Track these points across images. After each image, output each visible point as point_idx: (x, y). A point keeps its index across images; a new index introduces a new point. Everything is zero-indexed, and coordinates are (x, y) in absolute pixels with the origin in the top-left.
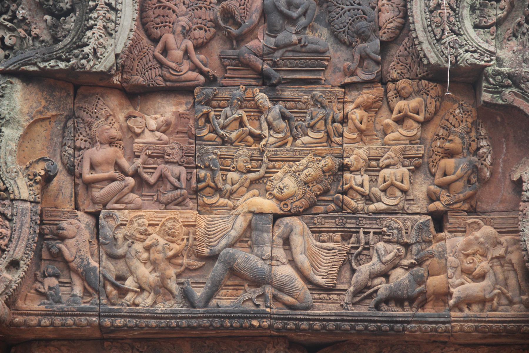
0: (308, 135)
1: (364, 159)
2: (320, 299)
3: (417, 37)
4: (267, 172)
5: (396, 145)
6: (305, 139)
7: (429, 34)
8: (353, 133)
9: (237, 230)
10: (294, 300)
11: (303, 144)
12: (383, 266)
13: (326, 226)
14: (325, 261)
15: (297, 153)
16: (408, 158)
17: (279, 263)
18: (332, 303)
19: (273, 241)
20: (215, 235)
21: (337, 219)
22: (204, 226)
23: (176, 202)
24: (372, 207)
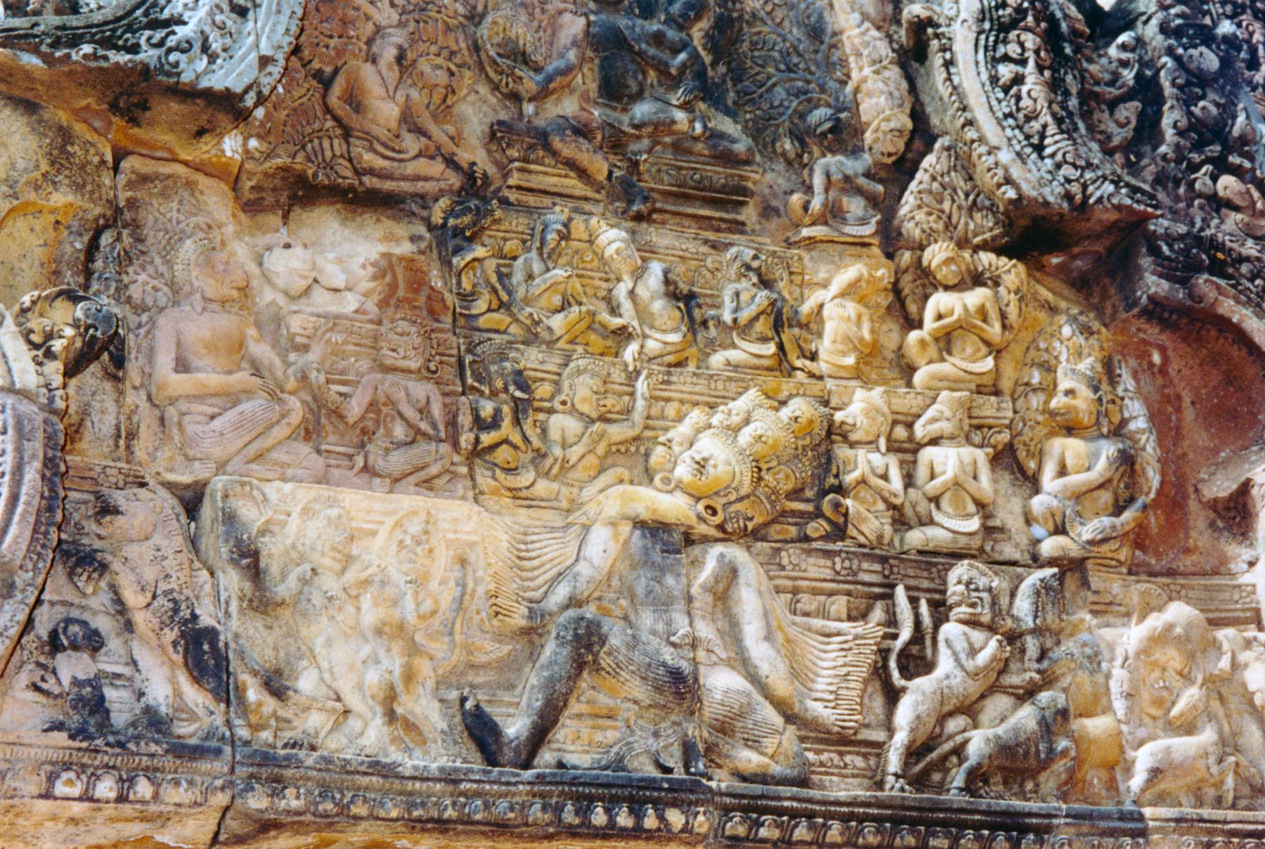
0: (734, 346)
1: (883, 415)
2: (822, 764)
3: (982, 140)
4: (646, 427)
5: (953, 390)
6: (733, 355)
7: (1009, 132)
8: (844, 354)
9: (596, 561)
10: (767, 760)
11: (729, 364)
12: (971, 682)
13: (811, 574)
14: (825, 664)
15: (720, 385)
16: (979, 427)
17: (714, 658)
18: (853, 776)
19: (690, 599)
20: (536, 573)
21: (837, 560)
22: (506, 545)
23: (423, 475)
24: (915, 538)
